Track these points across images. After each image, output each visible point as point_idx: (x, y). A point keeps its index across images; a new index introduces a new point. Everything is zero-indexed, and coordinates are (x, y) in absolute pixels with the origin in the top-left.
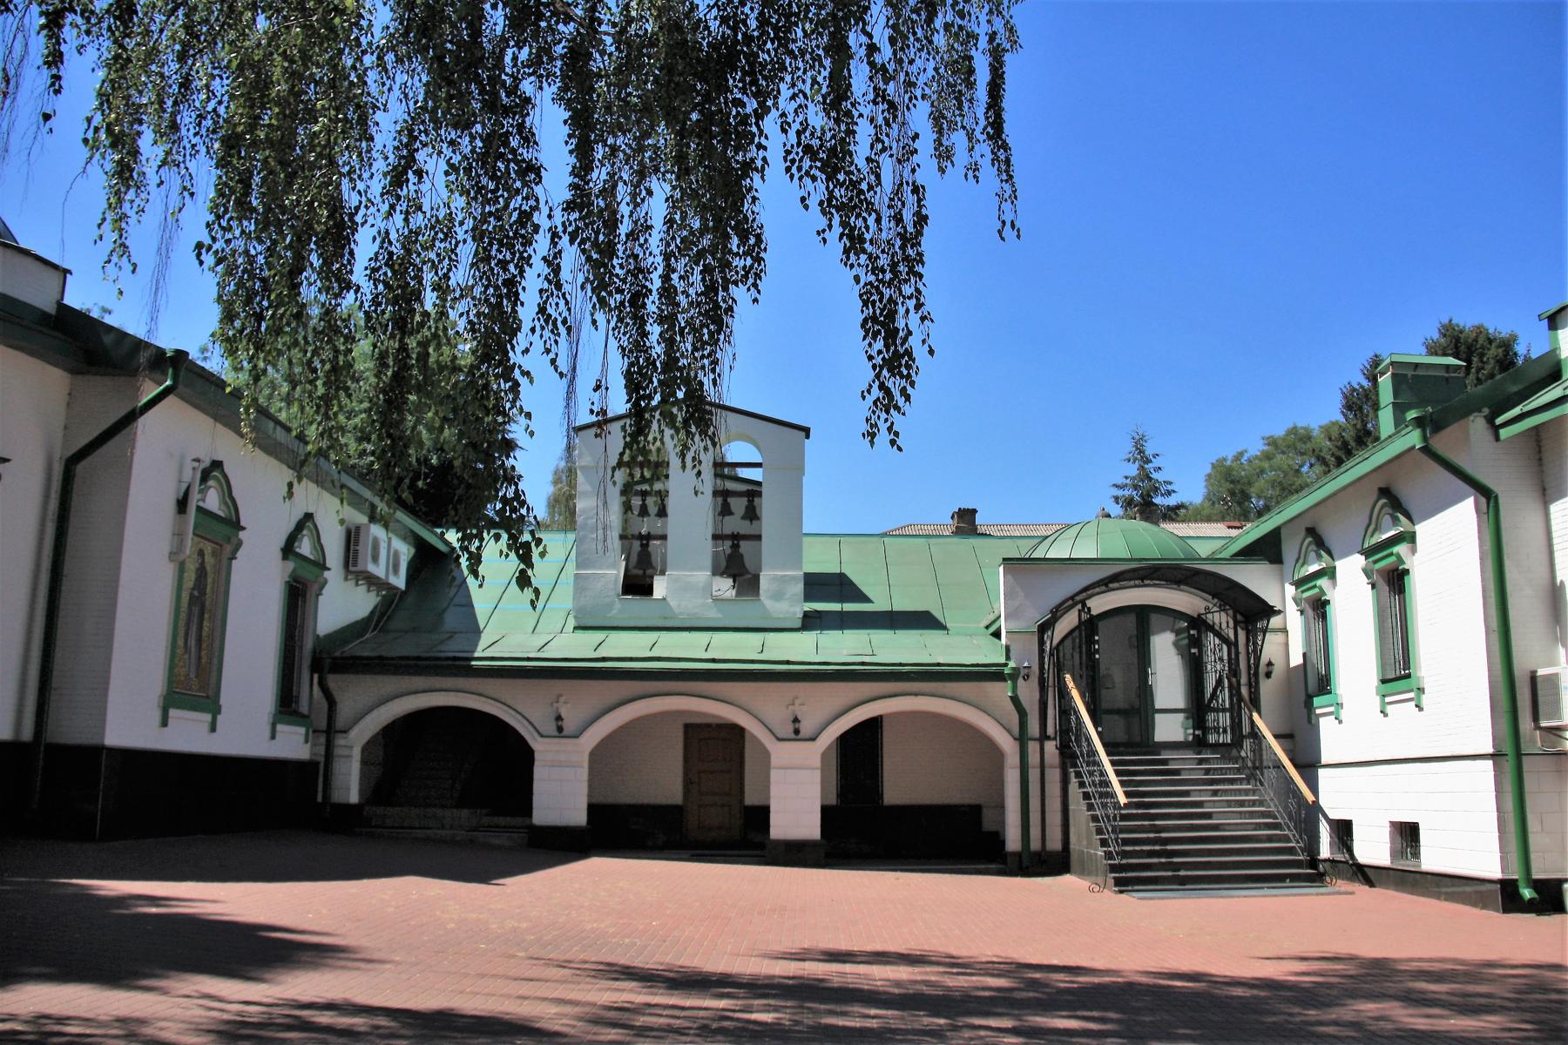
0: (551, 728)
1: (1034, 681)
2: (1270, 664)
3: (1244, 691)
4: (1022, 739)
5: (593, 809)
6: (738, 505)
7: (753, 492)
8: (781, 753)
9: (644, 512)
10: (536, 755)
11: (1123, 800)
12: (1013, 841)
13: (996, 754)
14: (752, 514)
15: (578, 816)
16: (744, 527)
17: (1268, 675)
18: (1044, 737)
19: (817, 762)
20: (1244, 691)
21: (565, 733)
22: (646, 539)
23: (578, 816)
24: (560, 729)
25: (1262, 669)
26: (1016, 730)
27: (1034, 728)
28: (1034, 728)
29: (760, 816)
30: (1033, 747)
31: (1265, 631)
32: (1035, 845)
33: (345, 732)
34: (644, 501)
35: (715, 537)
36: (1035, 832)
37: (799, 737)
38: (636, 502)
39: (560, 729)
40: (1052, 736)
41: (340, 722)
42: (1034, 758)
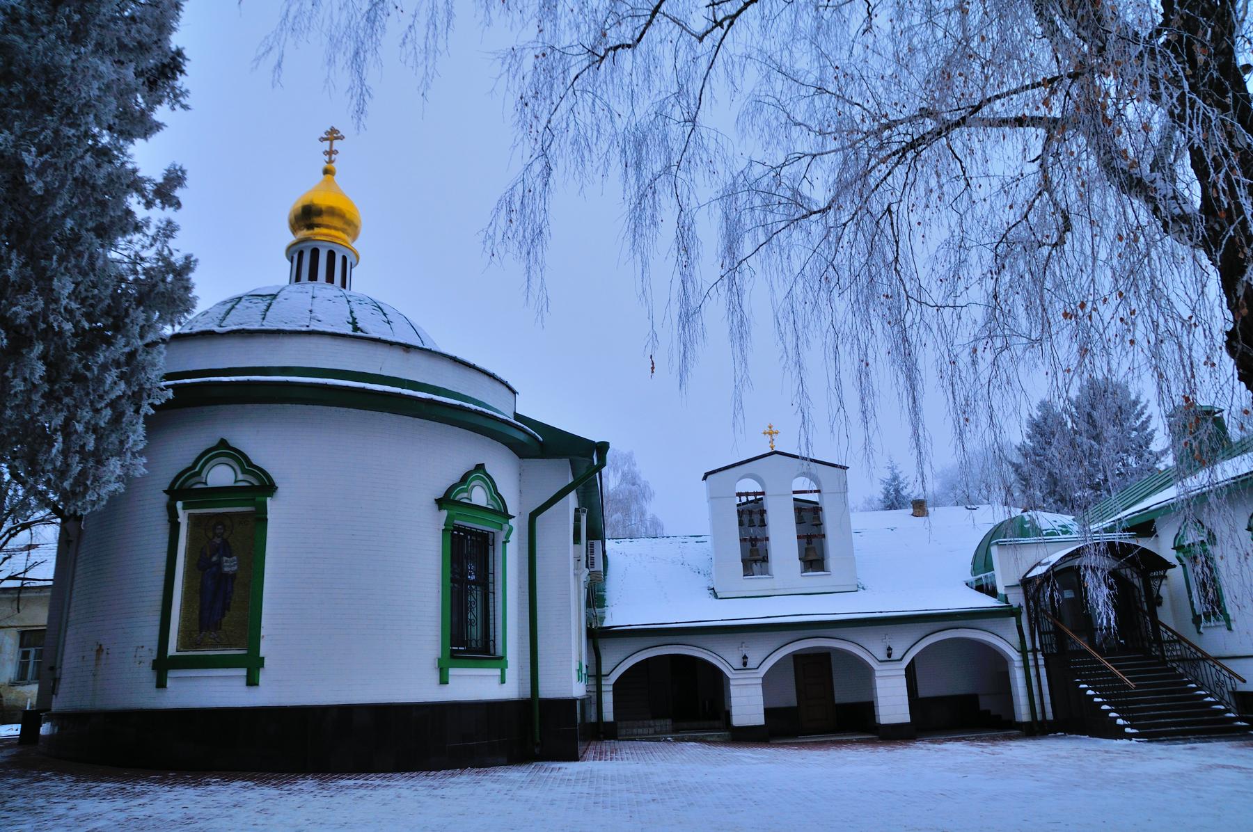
4: (1023, 651)
5: (768, 712)
6: (807, 516)
7: (816, 509)
8: (880, 671)
9: (752, 525)
10: (732, 682)
11: (1132, 685)
13: (1001, 661)
14: (819, 524)
15: (760, 720)
16: (814, 531)
19: (903, 672)
21: (747, 667)
22: (754, 541)
23: (760, 720)
24: (745, 664)
28: (1029, 646)
29: (869, 708)
30: (1030, 656)
32: (1039, 717)
33: (608, 675)
34: (751, 517)
35: (799, 537)
37: (892, 658)
38: (746, 519)
39: (745, 664)
40: (1039, 648)
41: (604, 672)
42: (1031, 663)
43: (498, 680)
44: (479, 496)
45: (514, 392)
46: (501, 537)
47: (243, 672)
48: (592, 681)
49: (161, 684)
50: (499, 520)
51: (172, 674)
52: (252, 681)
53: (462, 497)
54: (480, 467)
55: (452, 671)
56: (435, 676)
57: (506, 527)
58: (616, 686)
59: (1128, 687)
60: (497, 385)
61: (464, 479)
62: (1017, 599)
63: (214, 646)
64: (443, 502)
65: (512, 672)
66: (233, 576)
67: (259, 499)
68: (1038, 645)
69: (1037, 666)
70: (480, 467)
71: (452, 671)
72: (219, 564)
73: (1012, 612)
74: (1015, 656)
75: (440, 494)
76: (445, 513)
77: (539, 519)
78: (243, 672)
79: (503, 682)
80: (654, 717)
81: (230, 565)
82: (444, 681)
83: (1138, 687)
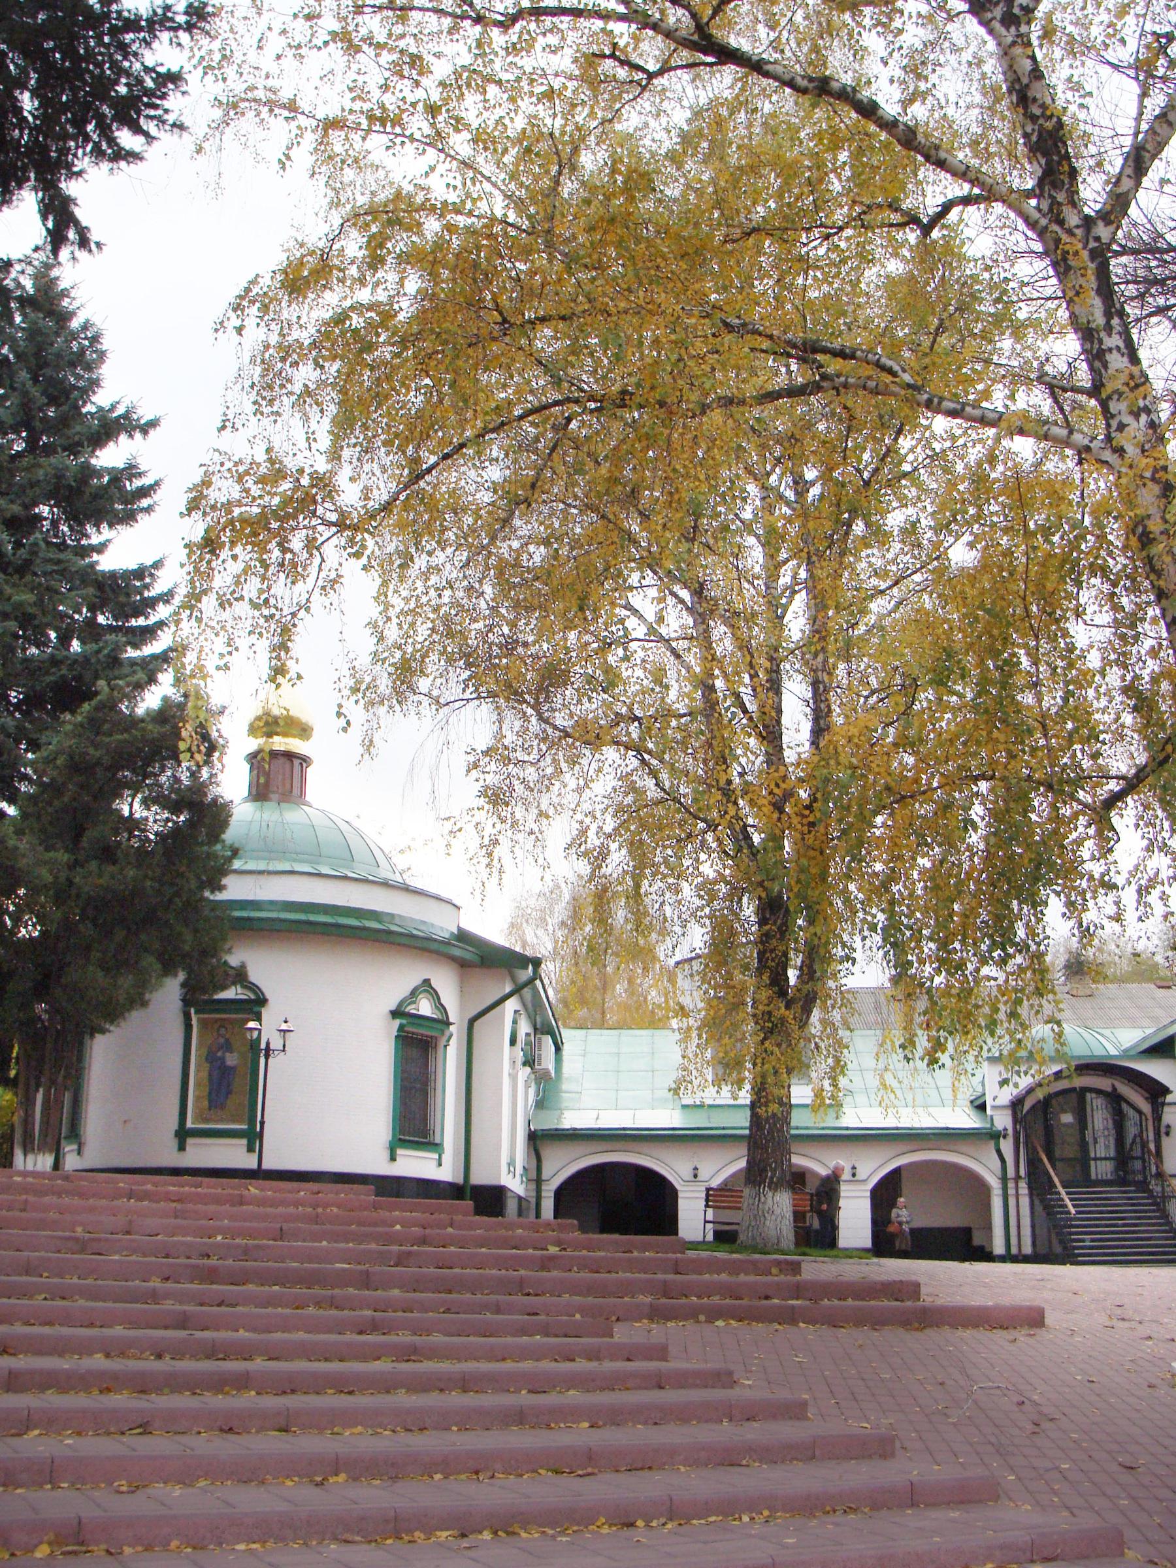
0: (688, 1176)
1: (1010, 1140)
2: (1168, 1126)
3: (1152, 1146)
4: (1004, 1179)
11: (1073, 1211)
12: (999, 1248)
17: (1167, 1134)
18: (1018, 1177)
20: (1152, 1146)
24: (695, 1176)
25: (1163, 1130)
26: (999, 1173)
27: (1011, 1172)
28: (1011, 1172)
30: (1011, 1185)
31: (1163, 1104)
36: (1014, 1240)
39: (695, 1176)
41: (545, 1176)
42: (1011, 1191)
43: (435, 1163)
44: (425, 1008)
45: (459, 908)
46: (442, 1042)
47: (244, 1141)
48: (533, 1186)
49: (182, 1148)
50: (439, 1026)
51: (190, 1141)
52: (250, 1149)
53: (411, 1009)
54: (427, 982)
55: (400, 1152)
56: (386, 1155)
57: (447, 1034)
58: (559, 1193)
59: (1069, 1212)
60: (444, 905)
61: (414, 993)
62: (1003, 1121)
63: (221, 1121)
64: (395, 1014)
65: (448, 1157)
66: (234, 1068)
67: (256, 1009)
68: (1022, 1172)
69: (1017, 1195)
70: (427, 982)
71: (400, 1152)
72: (223, 1059)
73: (995, 1136)
74: (994, 1182)
75: (393, 1008)
76: (397, 1022)
77: (476, 1024)
78: (244, 1141)
79: (440, 1165)
80: (602, 1231)
81: (231, 1060)
82: (393, 1158)
83: (1078, 1212)
